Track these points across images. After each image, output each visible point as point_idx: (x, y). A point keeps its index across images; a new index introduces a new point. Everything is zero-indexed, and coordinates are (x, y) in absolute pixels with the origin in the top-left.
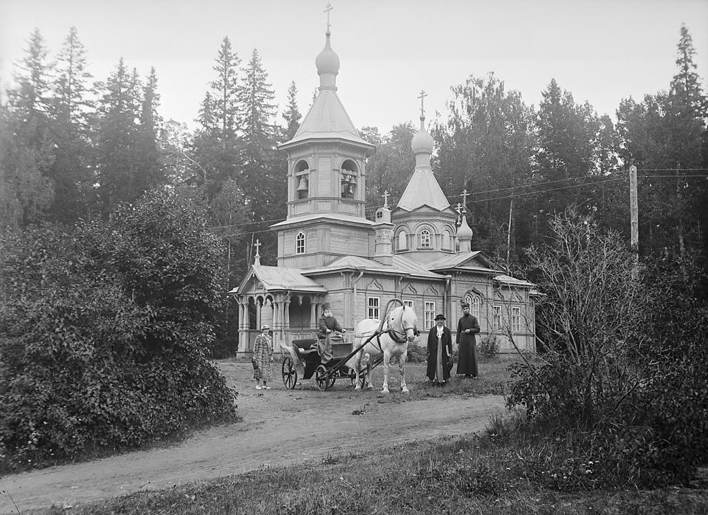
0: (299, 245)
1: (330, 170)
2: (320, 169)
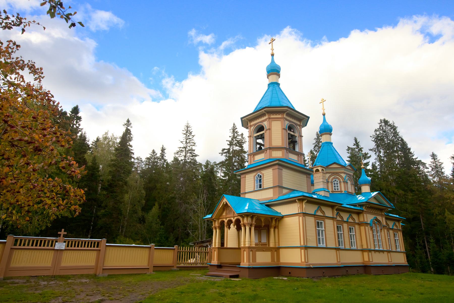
0: (257, 183)
1: (280, 129)
2: (273, 128)
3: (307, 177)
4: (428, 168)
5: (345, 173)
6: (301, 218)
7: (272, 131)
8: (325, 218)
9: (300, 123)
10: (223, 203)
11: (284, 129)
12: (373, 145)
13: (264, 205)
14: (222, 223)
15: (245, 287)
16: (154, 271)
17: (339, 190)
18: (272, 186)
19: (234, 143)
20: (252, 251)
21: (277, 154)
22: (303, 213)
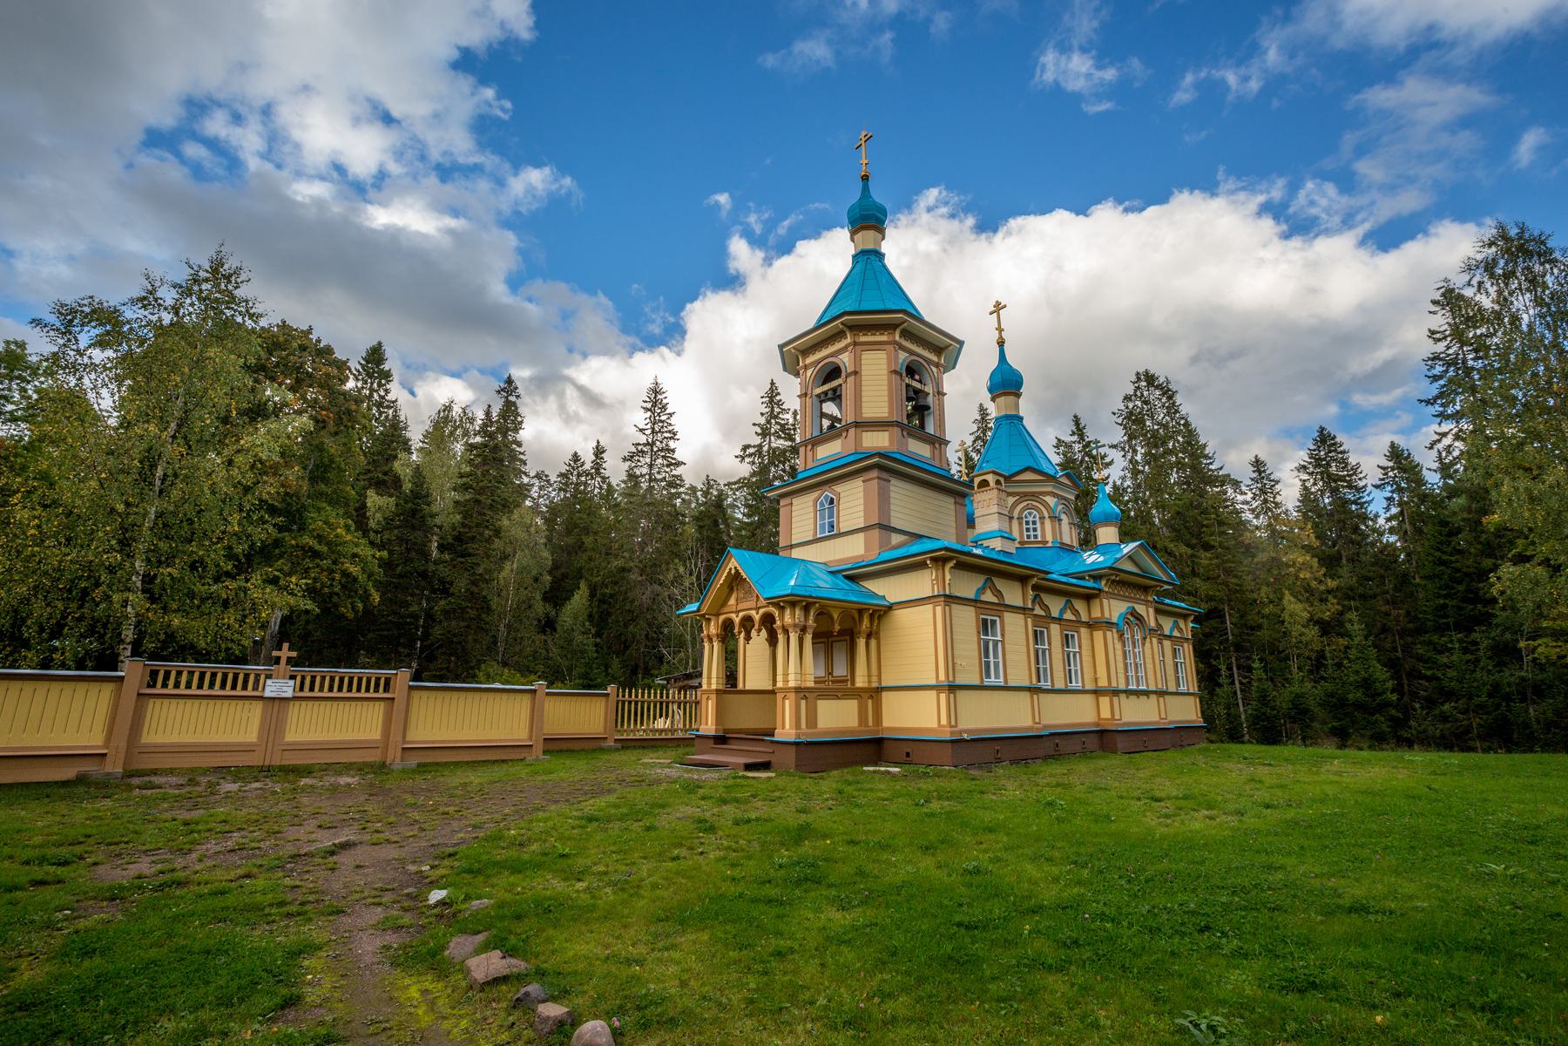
0: (823, 518)
1: (885, 372)
2: (865, 370)
3: (955, 503)
4: (1246, 494)
5: (1054, 495)
6: (939, 609)
7: (863, 378)
9: (939, 358)
10: (727, 571)
11: (895, 372)
12: (1119, 435)
13: (840, 576)
14: (728, 625)
15: (781, 798)
16: (545, 752)
17: (1039, 539)
18: (862, 526)
19: (773, 430)
20: (805, 698)
21: (877, 440)
22: (945, 596)
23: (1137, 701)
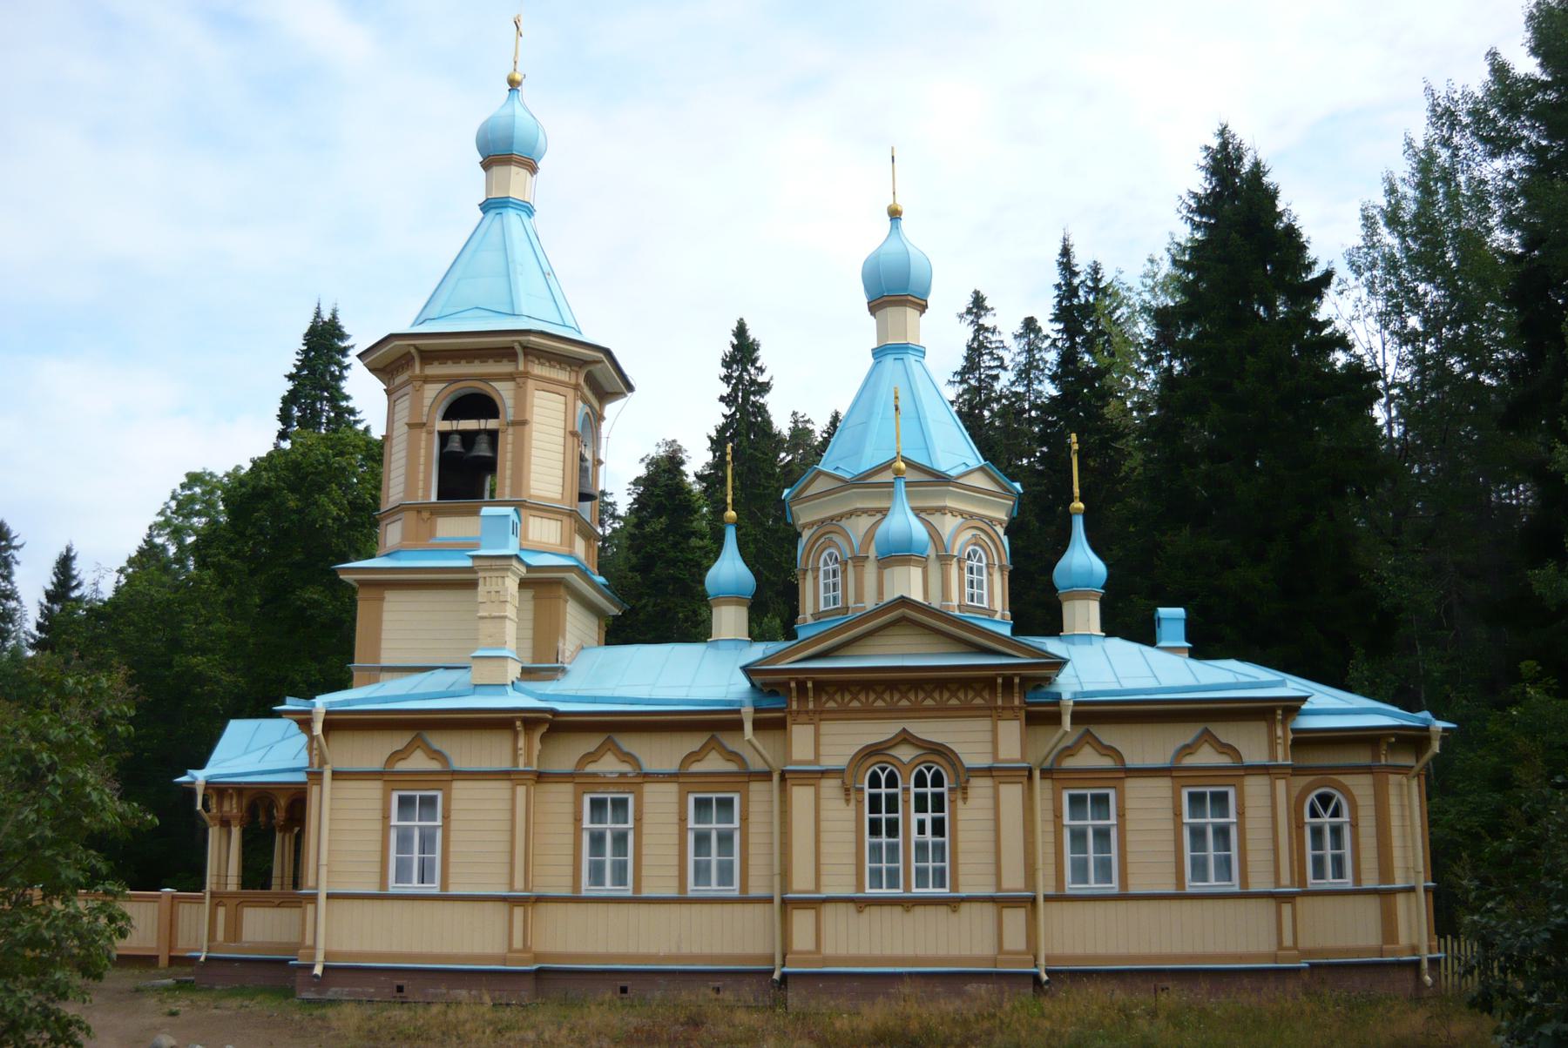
3: (535, 598)
8: (449, 778)
23: (954, 918)
